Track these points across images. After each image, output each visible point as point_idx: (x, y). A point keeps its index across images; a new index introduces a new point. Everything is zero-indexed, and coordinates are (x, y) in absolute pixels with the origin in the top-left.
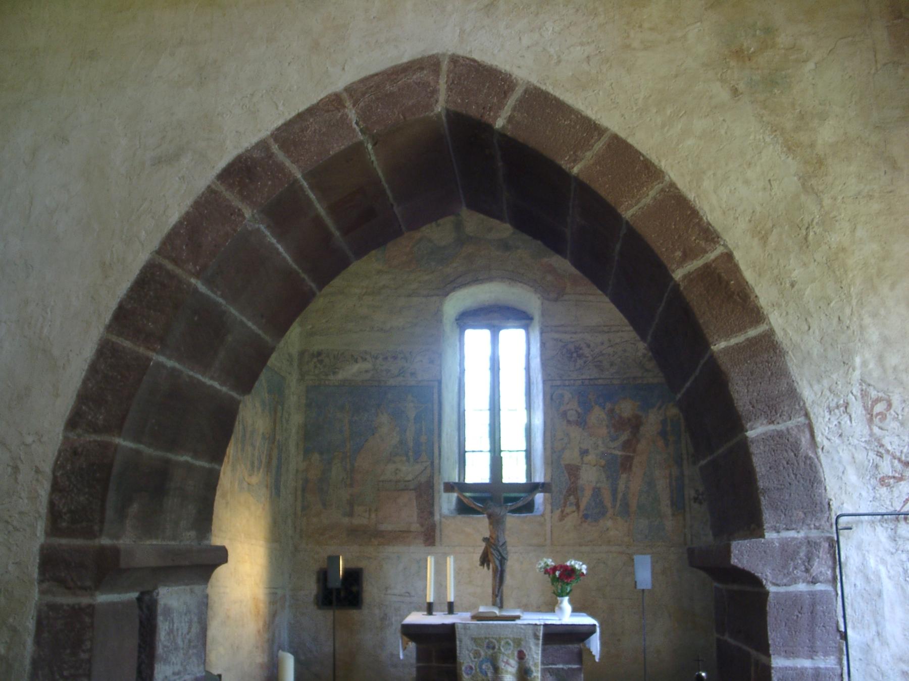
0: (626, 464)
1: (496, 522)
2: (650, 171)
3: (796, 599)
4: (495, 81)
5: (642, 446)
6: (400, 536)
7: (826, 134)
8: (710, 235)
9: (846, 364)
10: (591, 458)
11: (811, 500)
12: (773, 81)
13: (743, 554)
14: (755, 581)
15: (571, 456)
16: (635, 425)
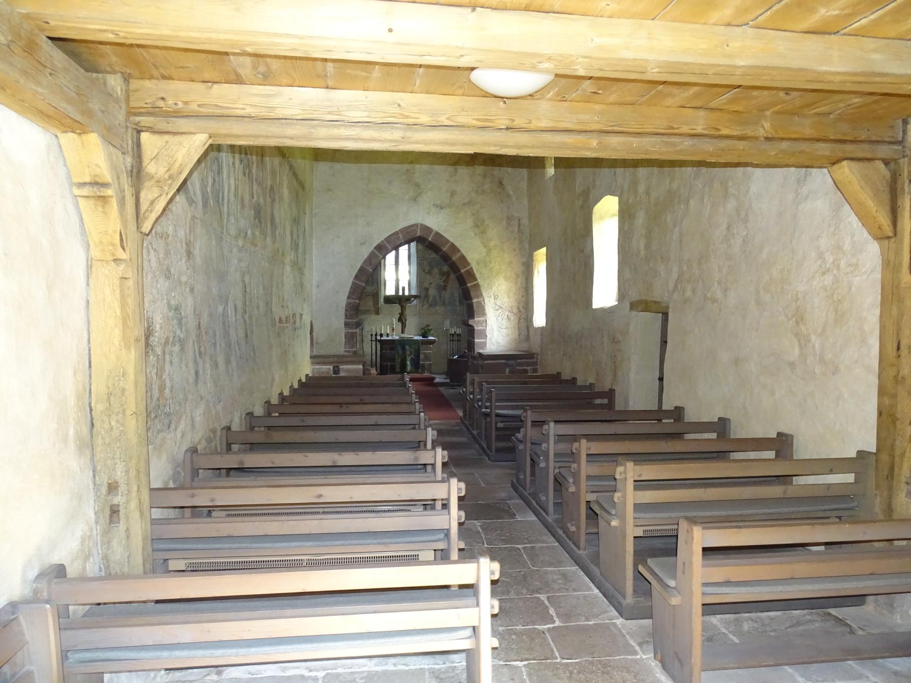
0: (445, 288)
1: (403, 308)
2: (459, 251)
3: (480, 330)
4: (427, 229)
5: (450, 282)
6: (367, 312)
7: (492, 244)
8: (469, 264)
9: (491, 289)
10: (433, 285)
11: (484, 314)
12: (483, 232)
13: (471, 322)
14: (472, 326)
15: (426, 285)
16: (447, 274)
